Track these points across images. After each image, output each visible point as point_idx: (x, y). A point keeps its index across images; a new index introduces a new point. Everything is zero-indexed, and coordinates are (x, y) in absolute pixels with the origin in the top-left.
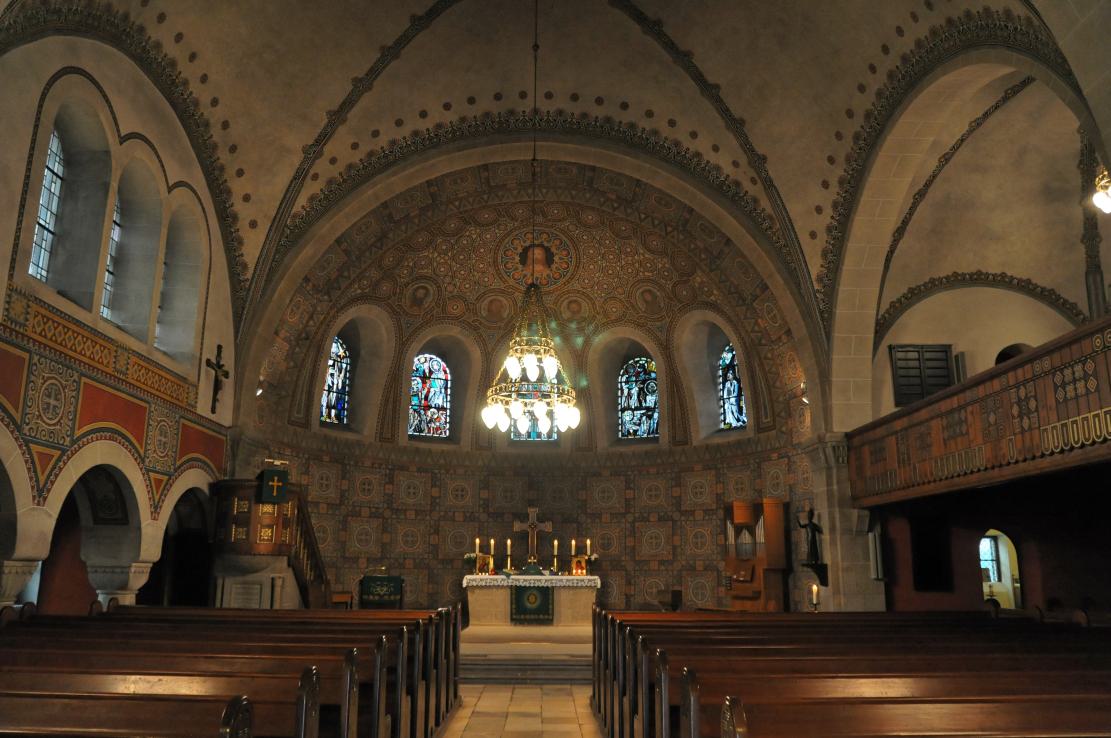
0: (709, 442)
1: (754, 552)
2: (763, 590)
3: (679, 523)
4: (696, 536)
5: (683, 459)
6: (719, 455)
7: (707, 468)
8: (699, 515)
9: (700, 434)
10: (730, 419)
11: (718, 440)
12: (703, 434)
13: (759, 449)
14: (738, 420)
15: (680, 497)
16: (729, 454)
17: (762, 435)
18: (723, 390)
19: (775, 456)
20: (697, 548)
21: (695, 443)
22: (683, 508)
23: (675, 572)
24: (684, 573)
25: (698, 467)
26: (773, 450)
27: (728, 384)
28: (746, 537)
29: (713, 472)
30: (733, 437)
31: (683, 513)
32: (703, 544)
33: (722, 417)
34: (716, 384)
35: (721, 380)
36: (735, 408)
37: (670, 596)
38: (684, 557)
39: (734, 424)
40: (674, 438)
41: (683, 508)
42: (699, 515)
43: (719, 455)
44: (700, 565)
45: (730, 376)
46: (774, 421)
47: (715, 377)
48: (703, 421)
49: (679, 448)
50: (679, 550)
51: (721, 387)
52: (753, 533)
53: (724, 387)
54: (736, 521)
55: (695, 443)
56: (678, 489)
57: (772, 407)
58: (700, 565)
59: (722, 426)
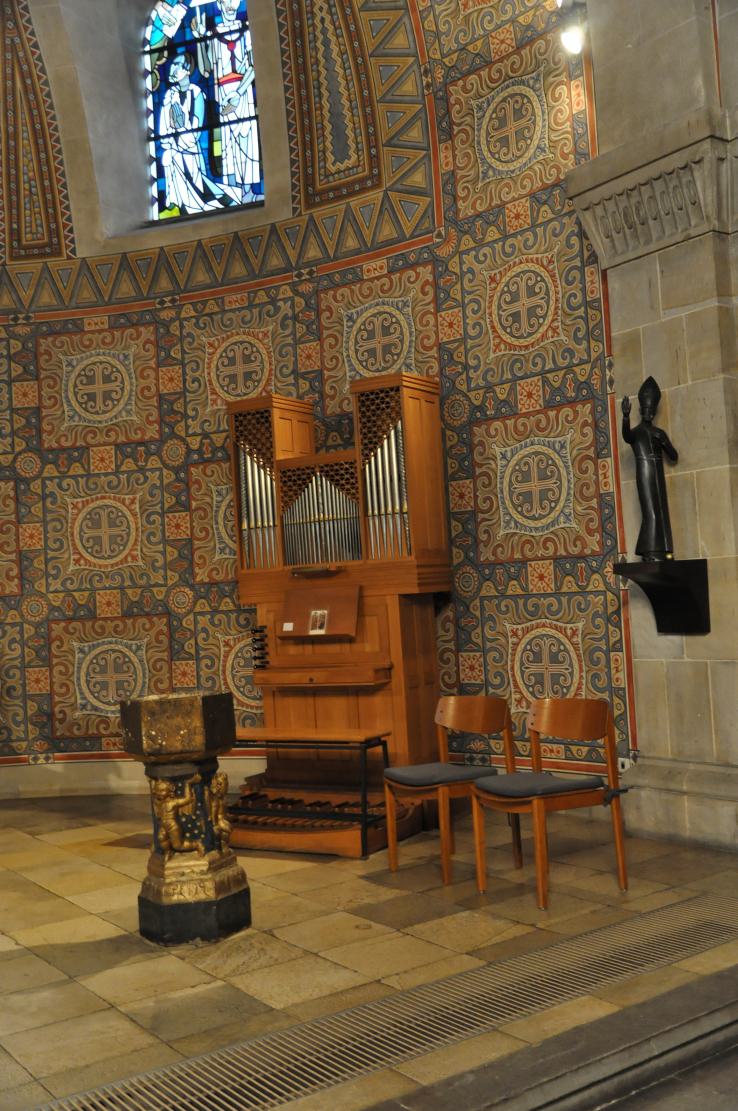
0: (130, 247)
1: (357, 543)
2: (396, 656)
3: (36, 486)
4: (94, 521)
5: (46, 298)
6: (164, 283)
7: (124, 321)
8: (102, 458)
9: (97, 229)
10: (181, 194)
11: (154, 241)
12: (108, 226)
13: (313, 252)
14: (207, 196)
15: (37, 411)
16: (202, 277)
17: (316, 212)
18: (156, 112)
19: (375, 266)
20: (98, 554)
21: (82, 252)
22: (49, 441)
23: (29, 630)
24: (57, 629)
25: (96, 321)
26: (375, 249)
27: (171, 97)
28: (323, 499)
29: (147, 333)
30: (188, 235)
31: (45, 455)
32: (118, 541)
33: (154, 191)
34: (137, 94)
35: (148, 83)
36: (196, 164)
37: (197, 722)
38: (56, 585)
39: (195, 205)
40: (16, 235)
41: (49, 441)
42: (102, 458)
43: (164, 283)
44: (107, 603)
45: (179, 72)
46: (375, 161)
47: (133, 74)
48: (106, 186)
49: (35, 266)
50: (39, 564)
51: (149, 103)
52: (347, 479)
53: (158, 104)
54: (280, 456)
55: (82, 252)
56: (30, 386)
57: (370, 120)
58: (107, 603)
59: (155, 214)
